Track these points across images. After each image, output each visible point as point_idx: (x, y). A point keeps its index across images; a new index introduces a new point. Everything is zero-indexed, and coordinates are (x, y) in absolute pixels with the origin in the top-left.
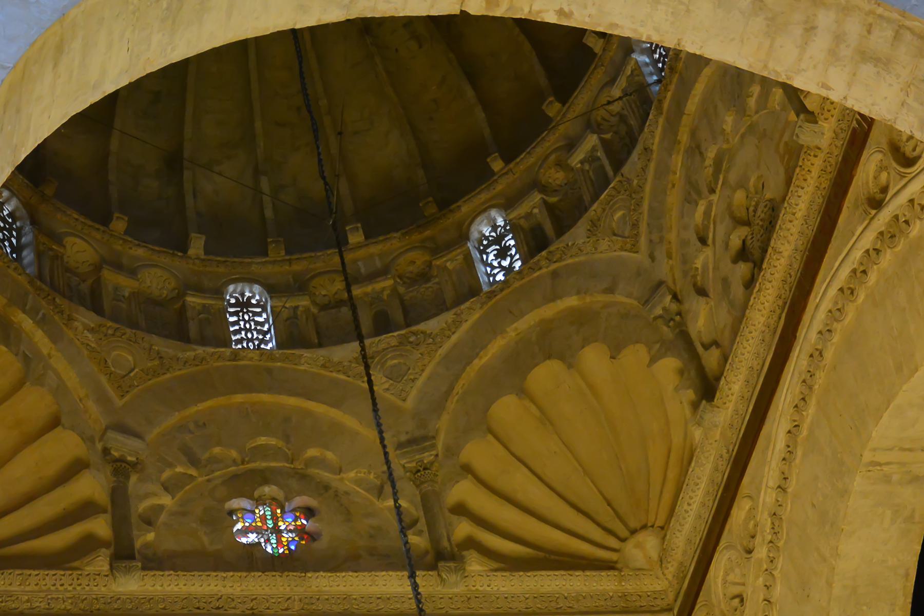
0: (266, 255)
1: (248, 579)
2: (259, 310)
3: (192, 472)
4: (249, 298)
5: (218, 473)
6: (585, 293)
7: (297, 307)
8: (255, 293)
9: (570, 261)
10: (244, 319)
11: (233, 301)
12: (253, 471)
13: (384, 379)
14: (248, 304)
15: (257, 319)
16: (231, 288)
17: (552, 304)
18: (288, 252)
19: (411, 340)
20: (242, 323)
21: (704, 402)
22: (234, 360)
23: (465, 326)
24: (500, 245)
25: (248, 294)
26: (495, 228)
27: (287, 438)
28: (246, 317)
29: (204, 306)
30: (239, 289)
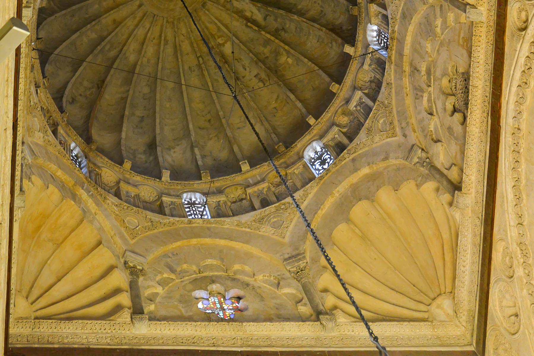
0: (201, 180)
1: (209, 326)
2: (200, 206)
3: (173, 276)
4: (194, 201)
5: (187, 278)
6: (373, 164)
7: (220, 201)
8: (197, 198)
9: (360, 152)
10: (193, 210)
11: (186, 202)
12: (205, 277)
13: (271, 229)
14: (194, 203)
15: (199, 209)
16: (185, 195)
17: (355, 174)
18: (212, 178)
19: (282, 207)
20: (192, 212)
21: (456, 192)
22: (190, 224)
23: (310, 196)
24: (321, 159)
25: (193, 199)
26: (316, 153)
27: (222, 260)
28: (194, 209)
29: (172, 202)
30: (189, 197)
